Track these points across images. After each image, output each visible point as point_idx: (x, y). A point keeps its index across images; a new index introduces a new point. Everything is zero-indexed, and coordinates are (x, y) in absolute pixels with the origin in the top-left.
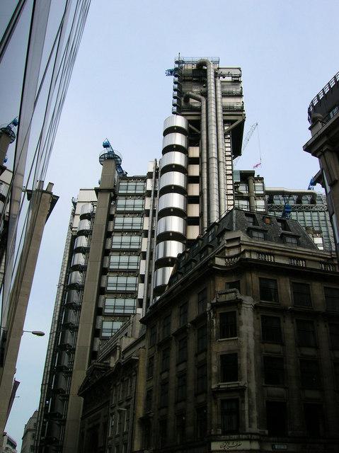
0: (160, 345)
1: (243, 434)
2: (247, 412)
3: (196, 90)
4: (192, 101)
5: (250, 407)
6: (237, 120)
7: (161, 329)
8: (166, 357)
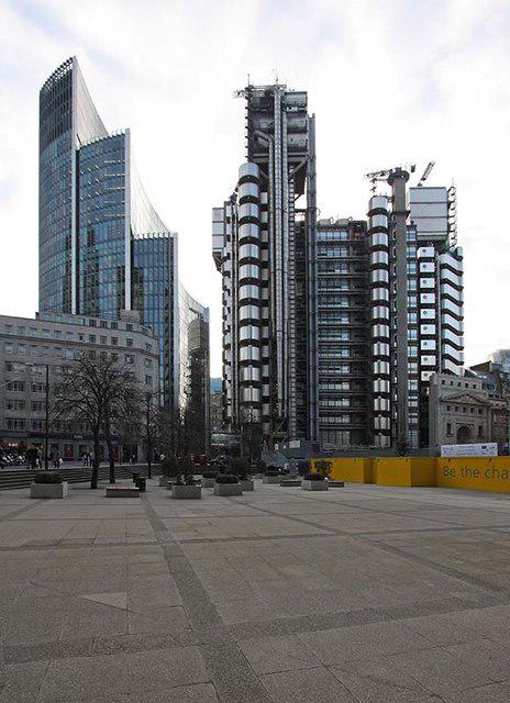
3: (264, 123)
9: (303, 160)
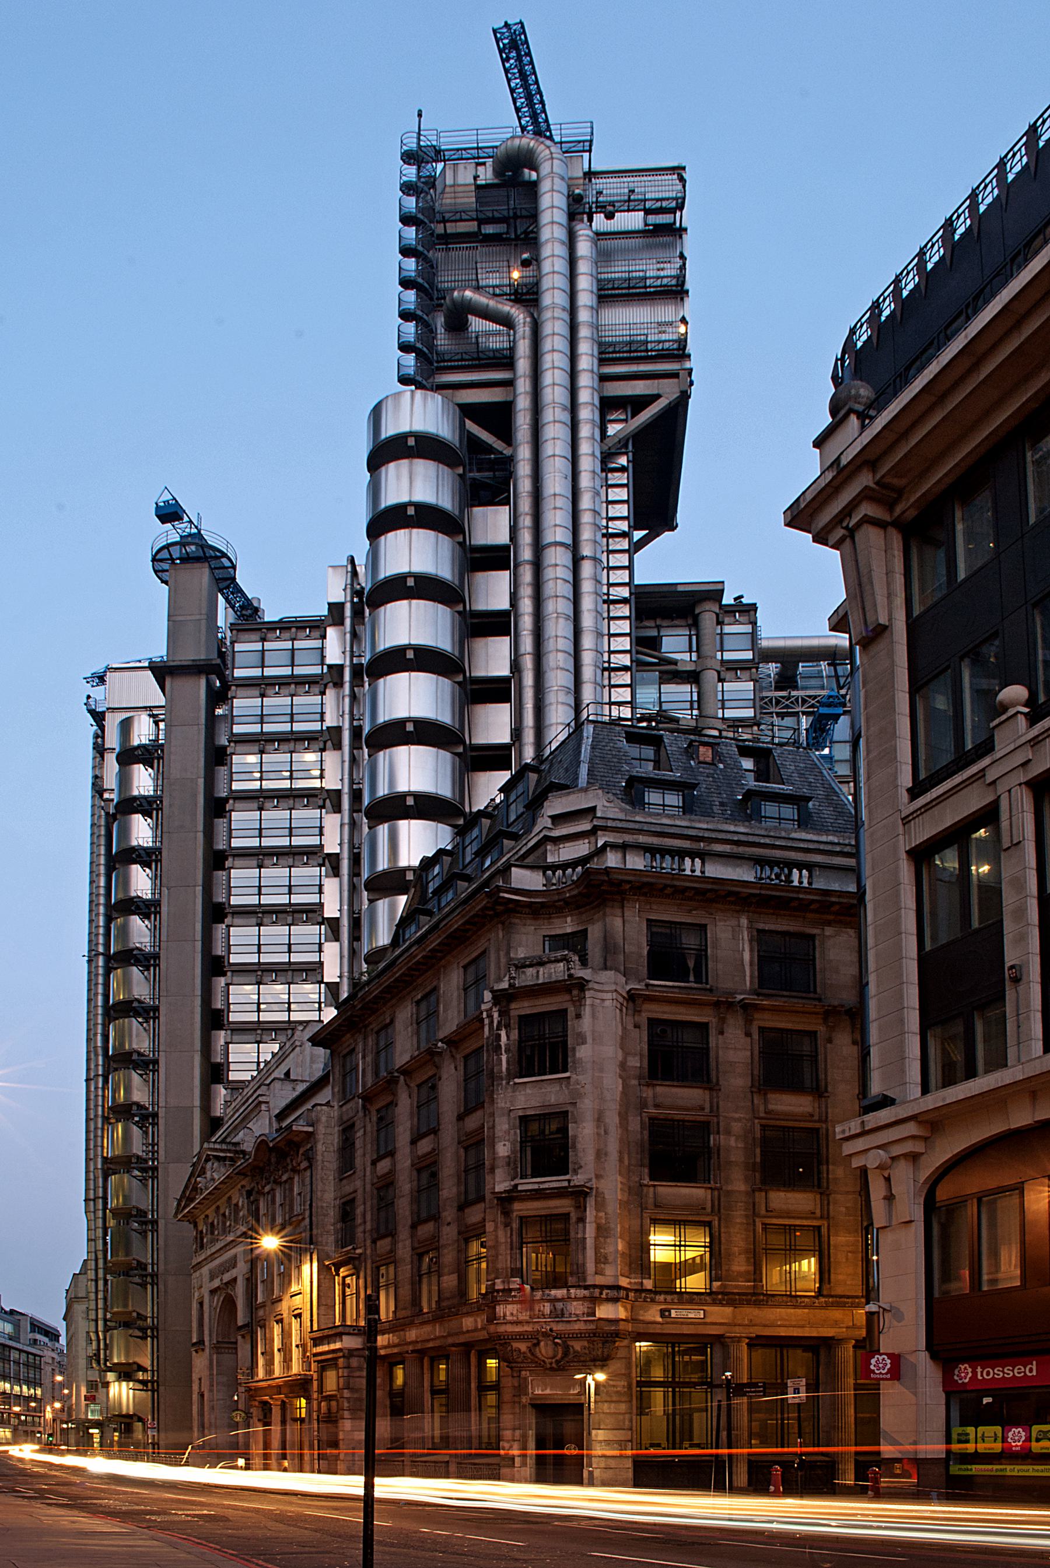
0: (367, 1098)
1: (578, 1287)
2: (590, 1242)
5: (602, 1231)
7: (369, 1059)
8: (385, 1123)
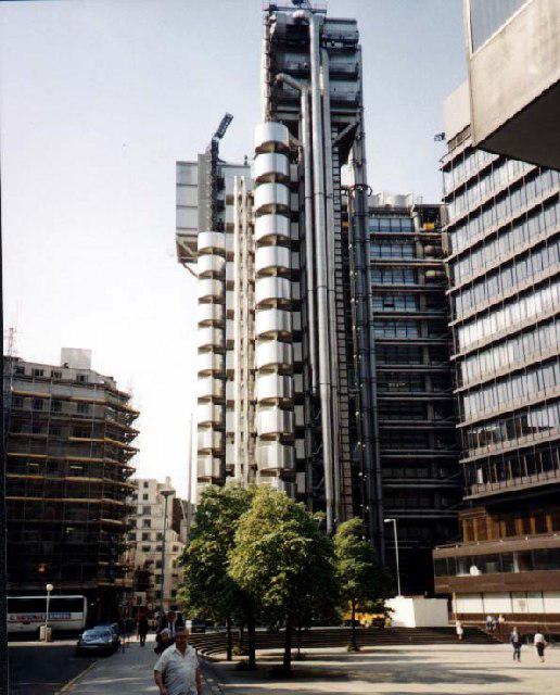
3: (293, 61)
4: (285, 87)
6: (346, 125)
9: (353, 121)
